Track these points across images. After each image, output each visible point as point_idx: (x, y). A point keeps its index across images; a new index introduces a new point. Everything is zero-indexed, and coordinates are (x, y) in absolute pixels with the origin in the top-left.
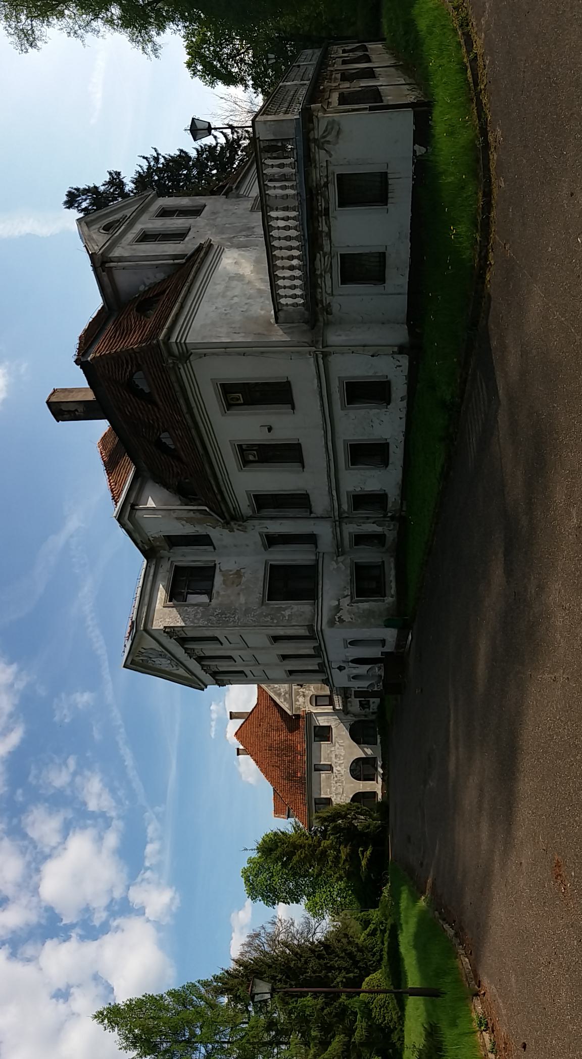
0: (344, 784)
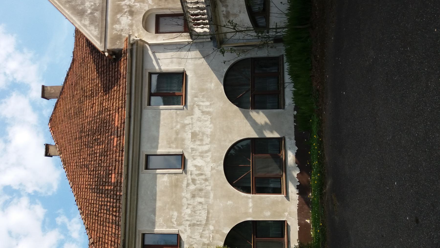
0: (211, 201)
